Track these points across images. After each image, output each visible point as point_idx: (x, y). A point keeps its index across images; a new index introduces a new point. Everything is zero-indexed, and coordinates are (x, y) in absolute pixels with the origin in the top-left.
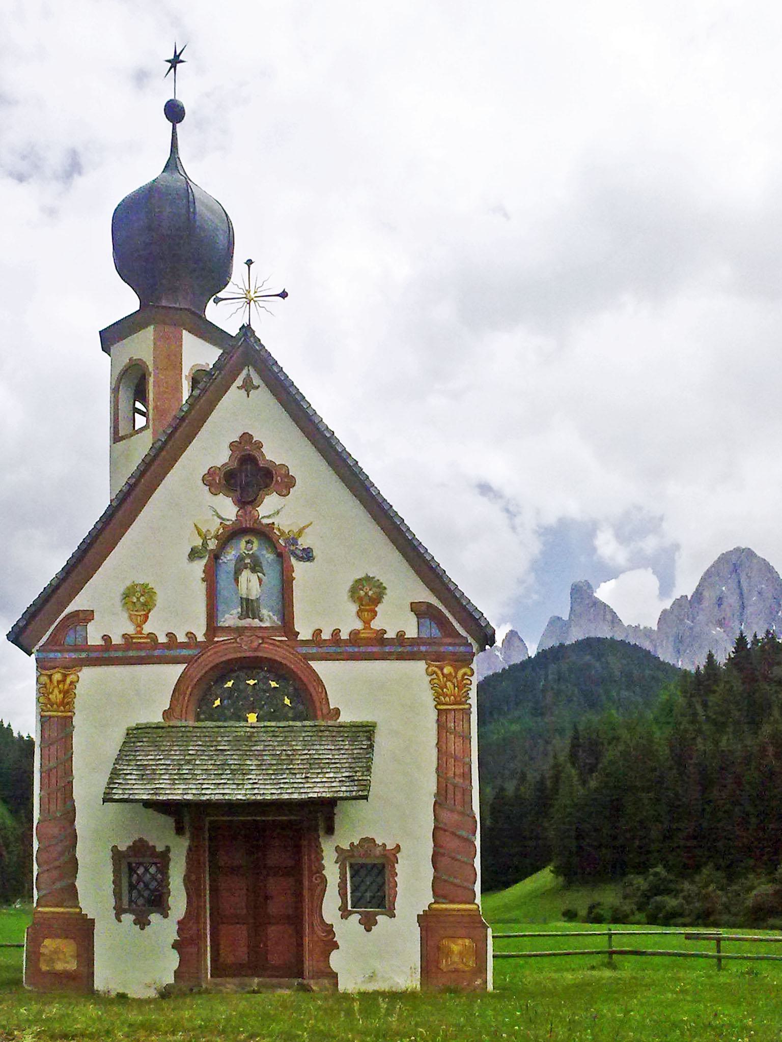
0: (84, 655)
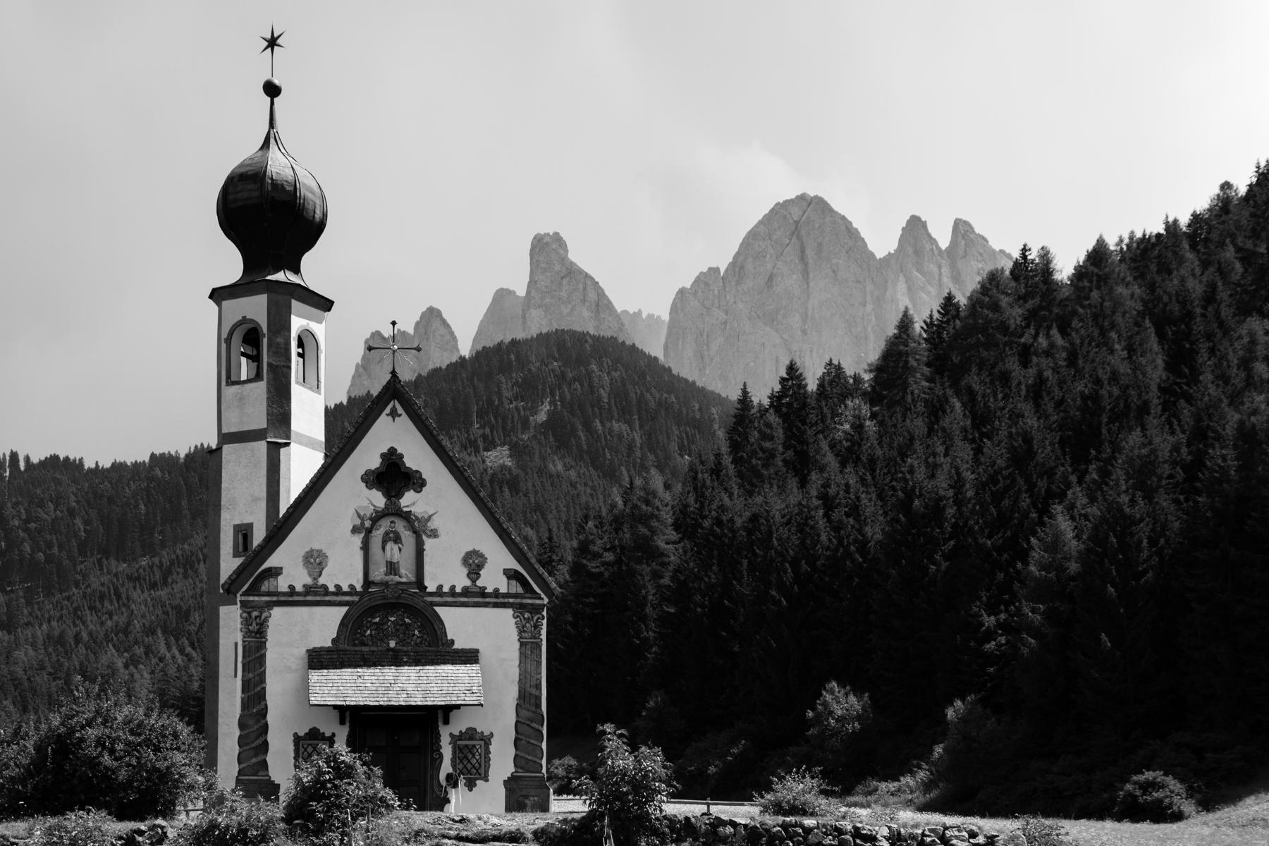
0: (275, 599)
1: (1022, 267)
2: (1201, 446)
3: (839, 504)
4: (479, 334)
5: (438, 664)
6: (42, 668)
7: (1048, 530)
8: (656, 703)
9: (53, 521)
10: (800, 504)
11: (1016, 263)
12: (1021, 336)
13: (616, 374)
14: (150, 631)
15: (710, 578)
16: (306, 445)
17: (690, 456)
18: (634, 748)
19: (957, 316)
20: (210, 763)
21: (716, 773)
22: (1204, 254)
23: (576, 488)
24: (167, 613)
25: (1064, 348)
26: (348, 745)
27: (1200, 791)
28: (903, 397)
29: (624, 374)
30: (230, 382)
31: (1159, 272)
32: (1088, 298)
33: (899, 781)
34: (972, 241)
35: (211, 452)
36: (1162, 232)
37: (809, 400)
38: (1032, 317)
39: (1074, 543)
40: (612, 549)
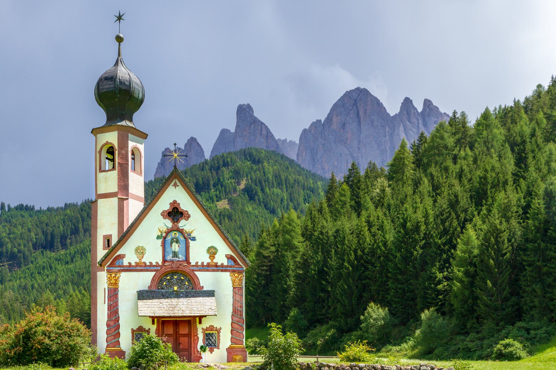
1: (453, 120)
2: (529, 199)
3: (374, 225)
4: (214, 149)
5: (196, 297)
6: (17, 300)
7: (465, 236)
8: (294, 313)
9: (21, 234)
10: (357, 225)
11: (451, 119)
12: (453, 151)
13: (275, 167)
14: (66, 283)
15: (318, 258)
16: (136, 199)
17: (308, 203)
18: (284, 333)
19: (425, 142)
20: (94, 342)
21: (321, 344)
22: (530, 115)
23: (258, 218)
24: (73, 275)
25: (472, 156)
26: (156, 334)
27: (528, 347)
28: (402, 177)
29: (279, 167)
30: (101, 171)
31: (512, 123)
32: (482, 134)
33: (401, 346)
34: (432, 108)
35: (92, 202)
36: (513, 105)
37: (361, 179)
38: (458, 142)
39: (476, 241)
40: (274, 245)
